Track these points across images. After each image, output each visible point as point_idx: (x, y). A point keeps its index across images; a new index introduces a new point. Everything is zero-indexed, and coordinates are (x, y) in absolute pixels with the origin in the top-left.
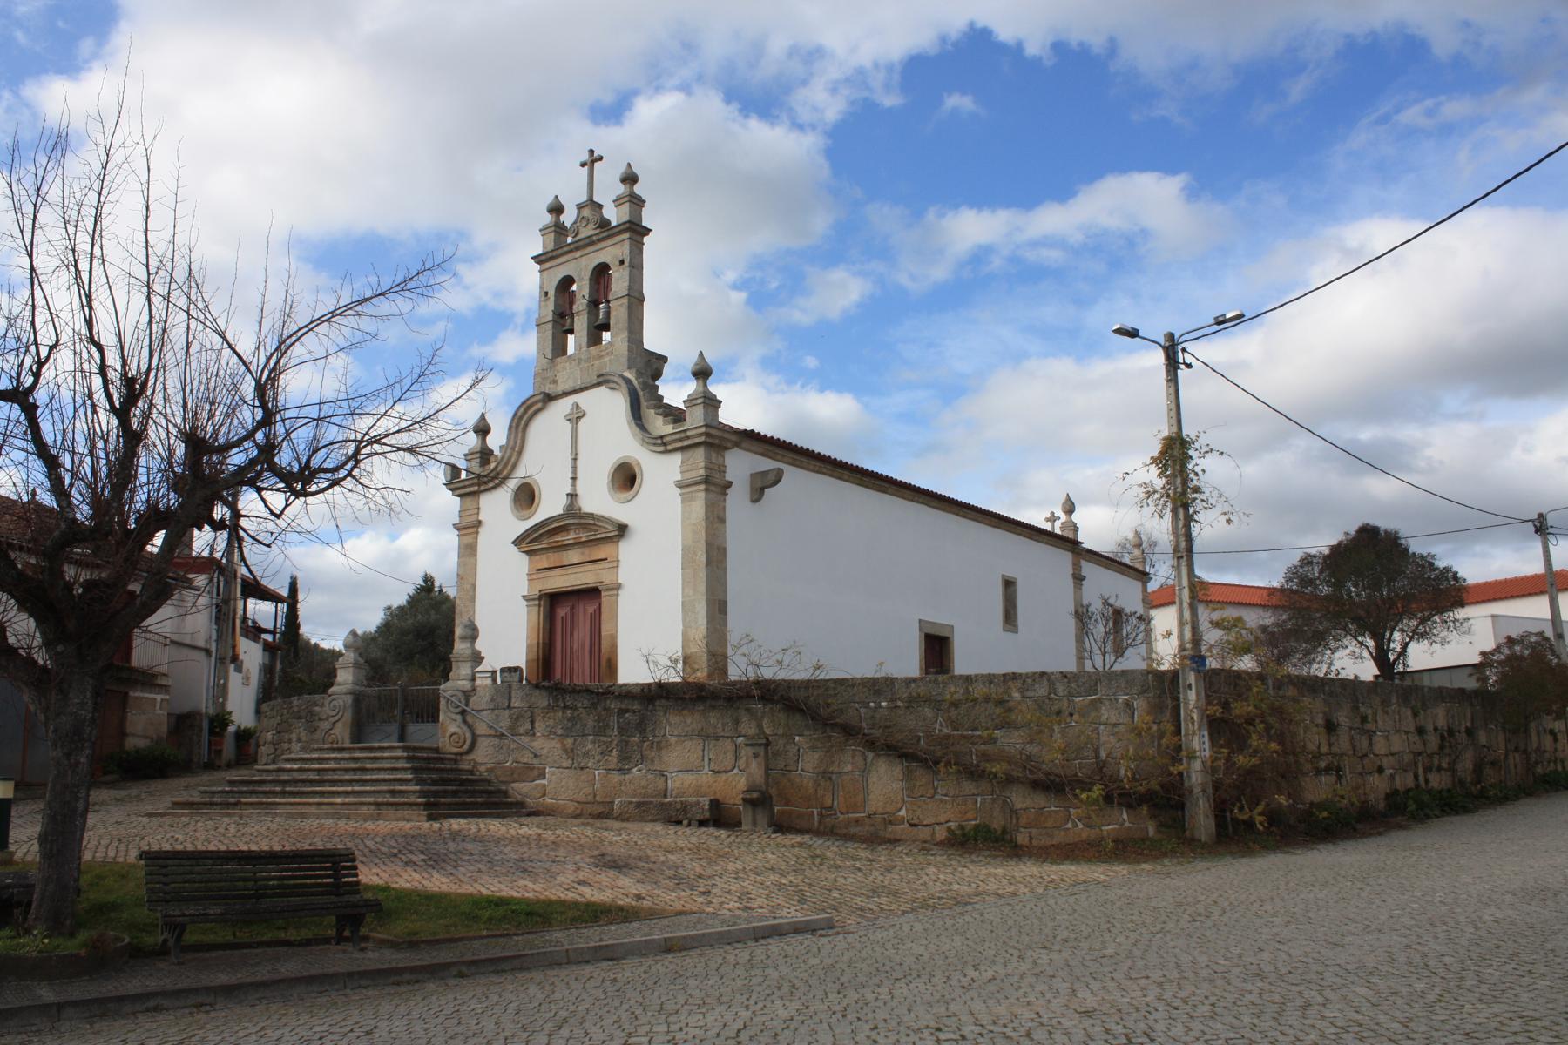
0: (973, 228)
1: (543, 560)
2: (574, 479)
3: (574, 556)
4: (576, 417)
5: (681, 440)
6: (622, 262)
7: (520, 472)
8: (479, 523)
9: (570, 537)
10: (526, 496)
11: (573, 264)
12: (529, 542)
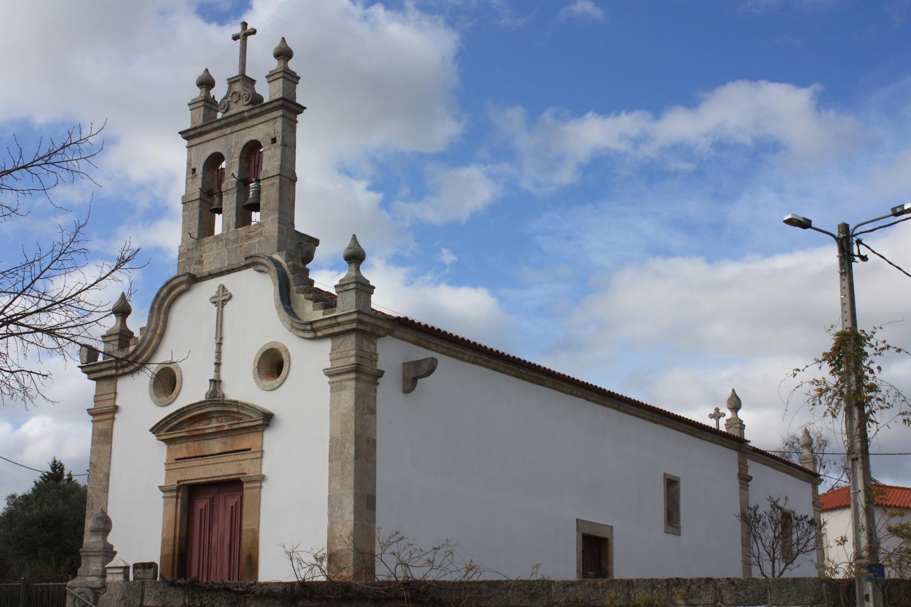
0: (594, 133)
1: (183, 450)
2: (218, 364)
3: (215, 446)
4: (222, 300)
5: (331, 326)
6: (274, 140)
7: (163, 357)
8: (116, 409)
9: (212, 425)
10: (167, 382)
11: (222, 141)
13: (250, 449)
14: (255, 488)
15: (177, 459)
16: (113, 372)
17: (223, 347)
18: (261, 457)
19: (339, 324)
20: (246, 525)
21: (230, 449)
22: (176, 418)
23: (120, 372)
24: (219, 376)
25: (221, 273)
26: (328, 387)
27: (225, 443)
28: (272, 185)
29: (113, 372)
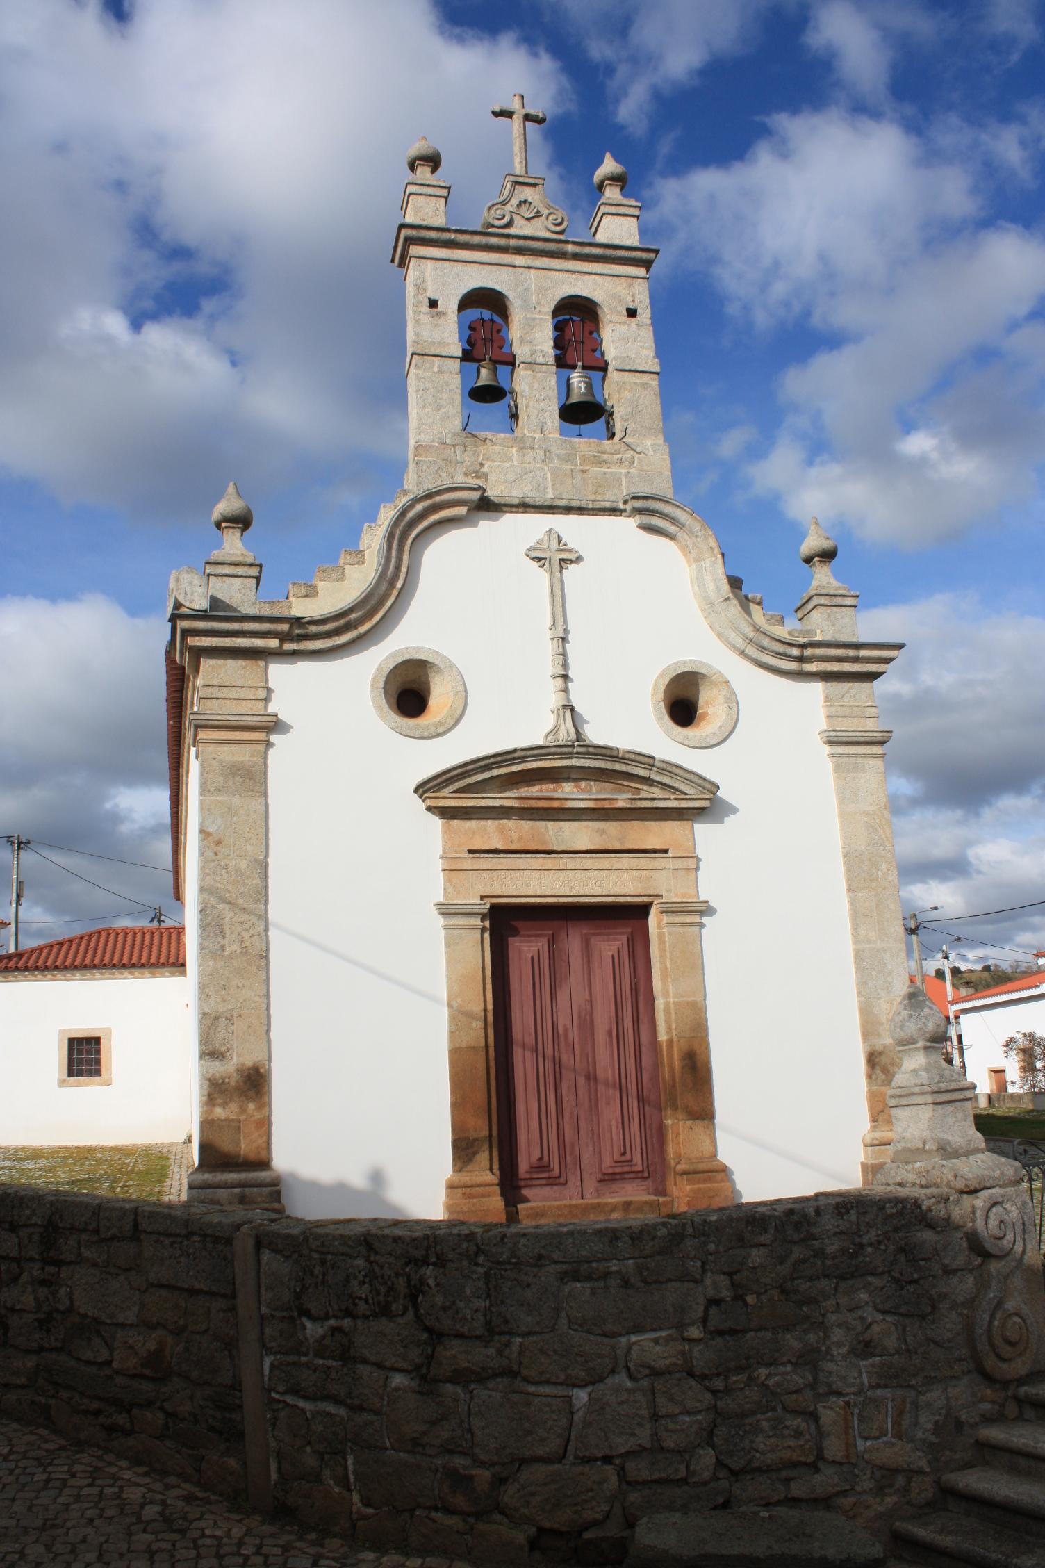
1: (490, 833)
2: (565, 677)
3: (580, 834)
4: (557, 560)
5: (840, 660)
6: (632, 313)
7: (404, 639)
9: (570, 793)
12: (460, 793)
13: (666, 851)
14: (691, 924)
15: (470, 851)
16: (274, 643)
18: (697, 869)
19: (856, 660)
20: (666, 994)
21: (617, 846)
22: (487, 768)
23: (289, 646)
24: (569, 700)
25: (550, 509)
26: (829, 765)
27: (602, 832)
28: (644, 386)
29: (274, 643)
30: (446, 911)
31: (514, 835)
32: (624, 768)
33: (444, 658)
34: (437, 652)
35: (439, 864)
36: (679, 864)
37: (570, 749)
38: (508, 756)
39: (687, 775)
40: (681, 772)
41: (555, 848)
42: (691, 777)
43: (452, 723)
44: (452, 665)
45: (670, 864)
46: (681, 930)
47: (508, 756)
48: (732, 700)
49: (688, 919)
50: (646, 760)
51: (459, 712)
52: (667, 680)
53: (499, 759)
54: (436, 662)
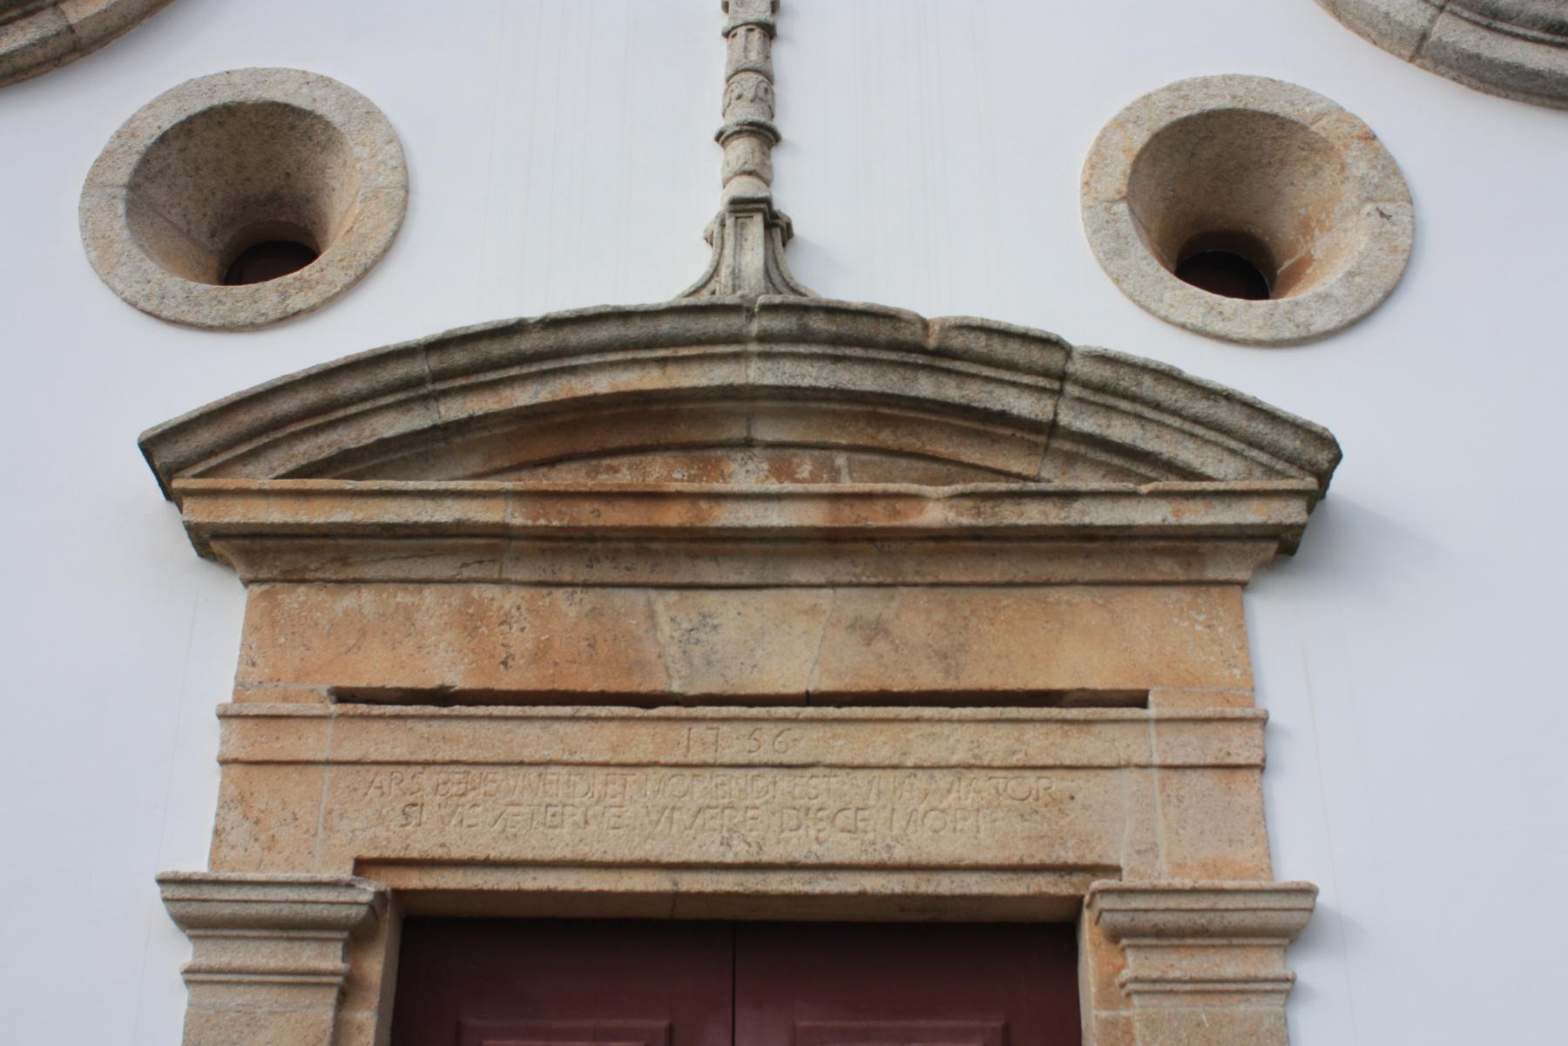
1: (425, 632)
2: (765, 135)
3: (784, 637)
9: (753, 490)
14: (1245, 987)
15: (343, 696)
17: (785, 57)
18: (1261, 767)
21: (930, 678)
22: (412, 392)
27: (874, 631)
30: (198, 908)
31: (521, 641)
32: (951, 391)
33: (350, 98)
34: (327, 82)
35: (210, 740)
36: (1190, 746)
37: (734, 323)
38: (496, 349)
39: (1201, 407)
40: (1179, 398)
41: (676, 687)
42: (1222, 413)
43: (342, 279)
44: (371, 114)
45: (1153, 746)
46: (1202, 1009)
47: (496, 349)
48: (1390, 190)
49: (1230, 965)
50: (1036, 355)
51: (373, 247)
52: (1140, 138)
53: (460, 357)
54: (321, 109)
